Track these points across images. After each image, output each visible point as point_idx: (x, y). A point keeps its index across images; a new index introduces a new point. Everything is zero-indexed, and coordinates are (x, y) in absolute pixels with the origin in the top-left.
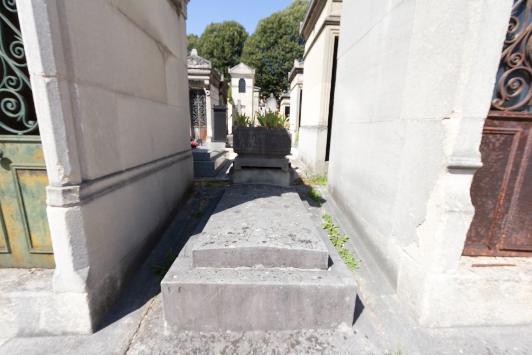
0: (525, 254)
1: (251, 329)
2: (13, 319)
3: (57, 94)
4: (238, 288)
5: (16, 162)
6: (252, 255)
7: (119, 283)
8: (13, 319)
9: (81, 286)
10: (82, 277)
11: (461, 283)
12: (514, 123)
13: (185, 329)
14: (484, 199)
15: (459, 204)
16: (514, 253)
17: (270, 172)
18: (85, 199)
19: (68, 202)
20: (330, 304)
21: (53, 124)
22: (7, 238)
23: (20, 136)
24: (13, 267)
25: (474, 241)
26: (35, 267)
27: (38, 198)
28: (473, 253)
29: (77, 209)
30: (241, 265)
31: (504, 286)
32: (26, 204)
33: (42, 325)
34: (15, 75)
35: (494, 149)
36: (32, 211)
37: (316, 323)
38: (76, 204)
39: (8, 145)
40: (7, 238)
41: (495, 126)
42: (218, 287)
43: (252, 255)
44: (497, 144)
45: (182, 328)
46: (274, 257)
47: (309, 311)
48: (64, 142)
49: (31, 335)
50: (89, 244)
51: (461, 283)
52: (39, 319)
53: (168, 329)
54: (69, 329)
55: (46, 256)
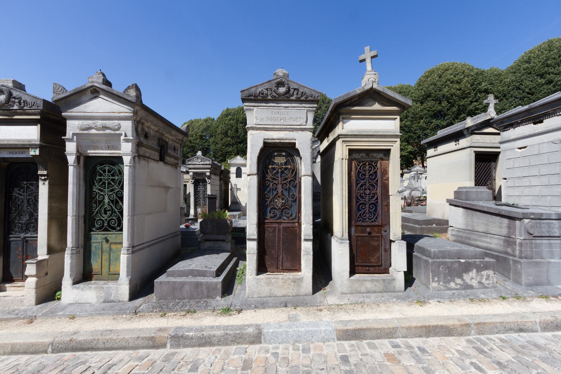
0: (291, 271)
1: (185, 299)
2: (103, 296)
3: (130, 220)
4: (180, 282)
5: (111, 241)
6: (188, 272)
7: (138, 288)
8: (103, 296)
9: (128, 282)
10: (128, 279)
11: (257, 280)
12: (275, 224)
13: (161, 299)
14: (271, 250)
15: (252, 251)
16: (287, 271)
17: (220, 242)
18: (133, 252)
19: (128, 253)
20: (212, 288)
21: (128, 229)
22: (102, 268)
23: (114, 232)
24: (101, 280)
25: (271, 266)
26: (109, 280)
27: (115, 253)
28: (271, 271)
29: (130, 255)
30: (184, 277)
31: (273, 281)
32: (111, 255)
33: (112, 298)
34: (116, 213)
35: (270, 232)
36: (112, 258)
37: (208, 296)
38: (130, 254)
39: (109, 235)
40: (102, 268)
41: (269, 225)
42: (174, 282)
43: (188, 272)
44: (271, 231)
45: (160, 299)
46: (196, 273)
47: (205, 291)
48: (130, 234)
49: (108, 302)
50: (132, 268)
51: (257, 280)
52: (111, 295)
53: (155, 299)
54: (121, 300)
55: (114, 275)
